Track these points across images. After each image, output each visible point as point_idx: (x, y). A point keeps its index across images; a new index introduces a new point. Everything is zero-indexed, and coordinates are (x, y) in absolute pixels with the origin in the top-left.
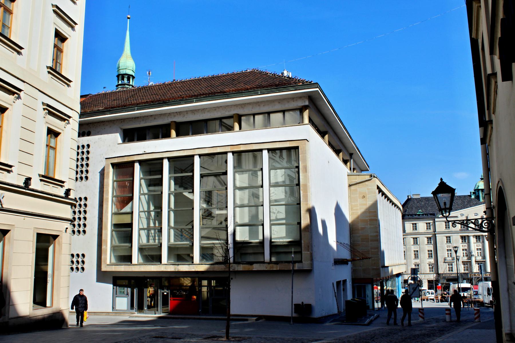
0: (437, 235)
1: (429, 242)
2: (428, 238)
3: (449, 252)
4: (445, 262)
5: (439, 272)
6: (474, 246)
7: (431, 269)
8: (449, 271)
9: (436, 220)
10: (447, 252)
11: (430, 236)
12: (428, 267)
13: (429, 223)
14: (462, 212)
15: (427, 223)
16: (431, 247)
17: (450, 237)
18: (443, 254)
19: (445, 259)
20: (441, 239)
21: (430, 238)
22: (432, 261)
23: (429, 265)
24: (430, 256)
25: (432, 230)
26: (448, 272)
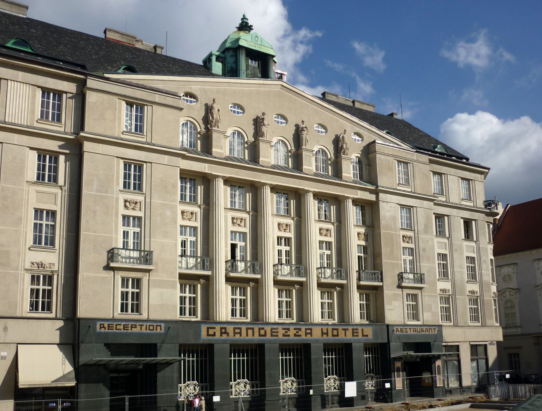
0: (87, 146)
1: (46, 175)
2: (42, 154)
3: (132, 230)
4: (107, 268)
5: (83, 312)
6: (226, 217)
7: (40, 302)
8: (124, 308)
9: (91, 83)
10: (121, 229)
11: (53, 145)
12: (28, 286)
13: (59, 94)
14: (194, 89)
15: (46, 91)
16: (55, 198)
17: (139, 167)
18: (103, 229)
19: (112, 254)
20: (102, 166)
21: (54, 156)
22: (53, 259)
23: (35, 279)
24: (43, 239)
25: (66, 127)
26: (118, 313)
